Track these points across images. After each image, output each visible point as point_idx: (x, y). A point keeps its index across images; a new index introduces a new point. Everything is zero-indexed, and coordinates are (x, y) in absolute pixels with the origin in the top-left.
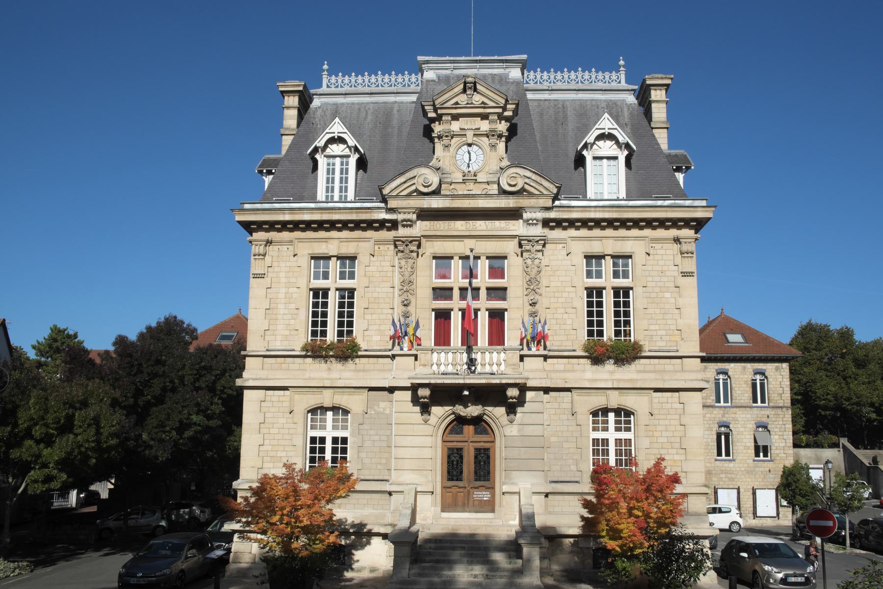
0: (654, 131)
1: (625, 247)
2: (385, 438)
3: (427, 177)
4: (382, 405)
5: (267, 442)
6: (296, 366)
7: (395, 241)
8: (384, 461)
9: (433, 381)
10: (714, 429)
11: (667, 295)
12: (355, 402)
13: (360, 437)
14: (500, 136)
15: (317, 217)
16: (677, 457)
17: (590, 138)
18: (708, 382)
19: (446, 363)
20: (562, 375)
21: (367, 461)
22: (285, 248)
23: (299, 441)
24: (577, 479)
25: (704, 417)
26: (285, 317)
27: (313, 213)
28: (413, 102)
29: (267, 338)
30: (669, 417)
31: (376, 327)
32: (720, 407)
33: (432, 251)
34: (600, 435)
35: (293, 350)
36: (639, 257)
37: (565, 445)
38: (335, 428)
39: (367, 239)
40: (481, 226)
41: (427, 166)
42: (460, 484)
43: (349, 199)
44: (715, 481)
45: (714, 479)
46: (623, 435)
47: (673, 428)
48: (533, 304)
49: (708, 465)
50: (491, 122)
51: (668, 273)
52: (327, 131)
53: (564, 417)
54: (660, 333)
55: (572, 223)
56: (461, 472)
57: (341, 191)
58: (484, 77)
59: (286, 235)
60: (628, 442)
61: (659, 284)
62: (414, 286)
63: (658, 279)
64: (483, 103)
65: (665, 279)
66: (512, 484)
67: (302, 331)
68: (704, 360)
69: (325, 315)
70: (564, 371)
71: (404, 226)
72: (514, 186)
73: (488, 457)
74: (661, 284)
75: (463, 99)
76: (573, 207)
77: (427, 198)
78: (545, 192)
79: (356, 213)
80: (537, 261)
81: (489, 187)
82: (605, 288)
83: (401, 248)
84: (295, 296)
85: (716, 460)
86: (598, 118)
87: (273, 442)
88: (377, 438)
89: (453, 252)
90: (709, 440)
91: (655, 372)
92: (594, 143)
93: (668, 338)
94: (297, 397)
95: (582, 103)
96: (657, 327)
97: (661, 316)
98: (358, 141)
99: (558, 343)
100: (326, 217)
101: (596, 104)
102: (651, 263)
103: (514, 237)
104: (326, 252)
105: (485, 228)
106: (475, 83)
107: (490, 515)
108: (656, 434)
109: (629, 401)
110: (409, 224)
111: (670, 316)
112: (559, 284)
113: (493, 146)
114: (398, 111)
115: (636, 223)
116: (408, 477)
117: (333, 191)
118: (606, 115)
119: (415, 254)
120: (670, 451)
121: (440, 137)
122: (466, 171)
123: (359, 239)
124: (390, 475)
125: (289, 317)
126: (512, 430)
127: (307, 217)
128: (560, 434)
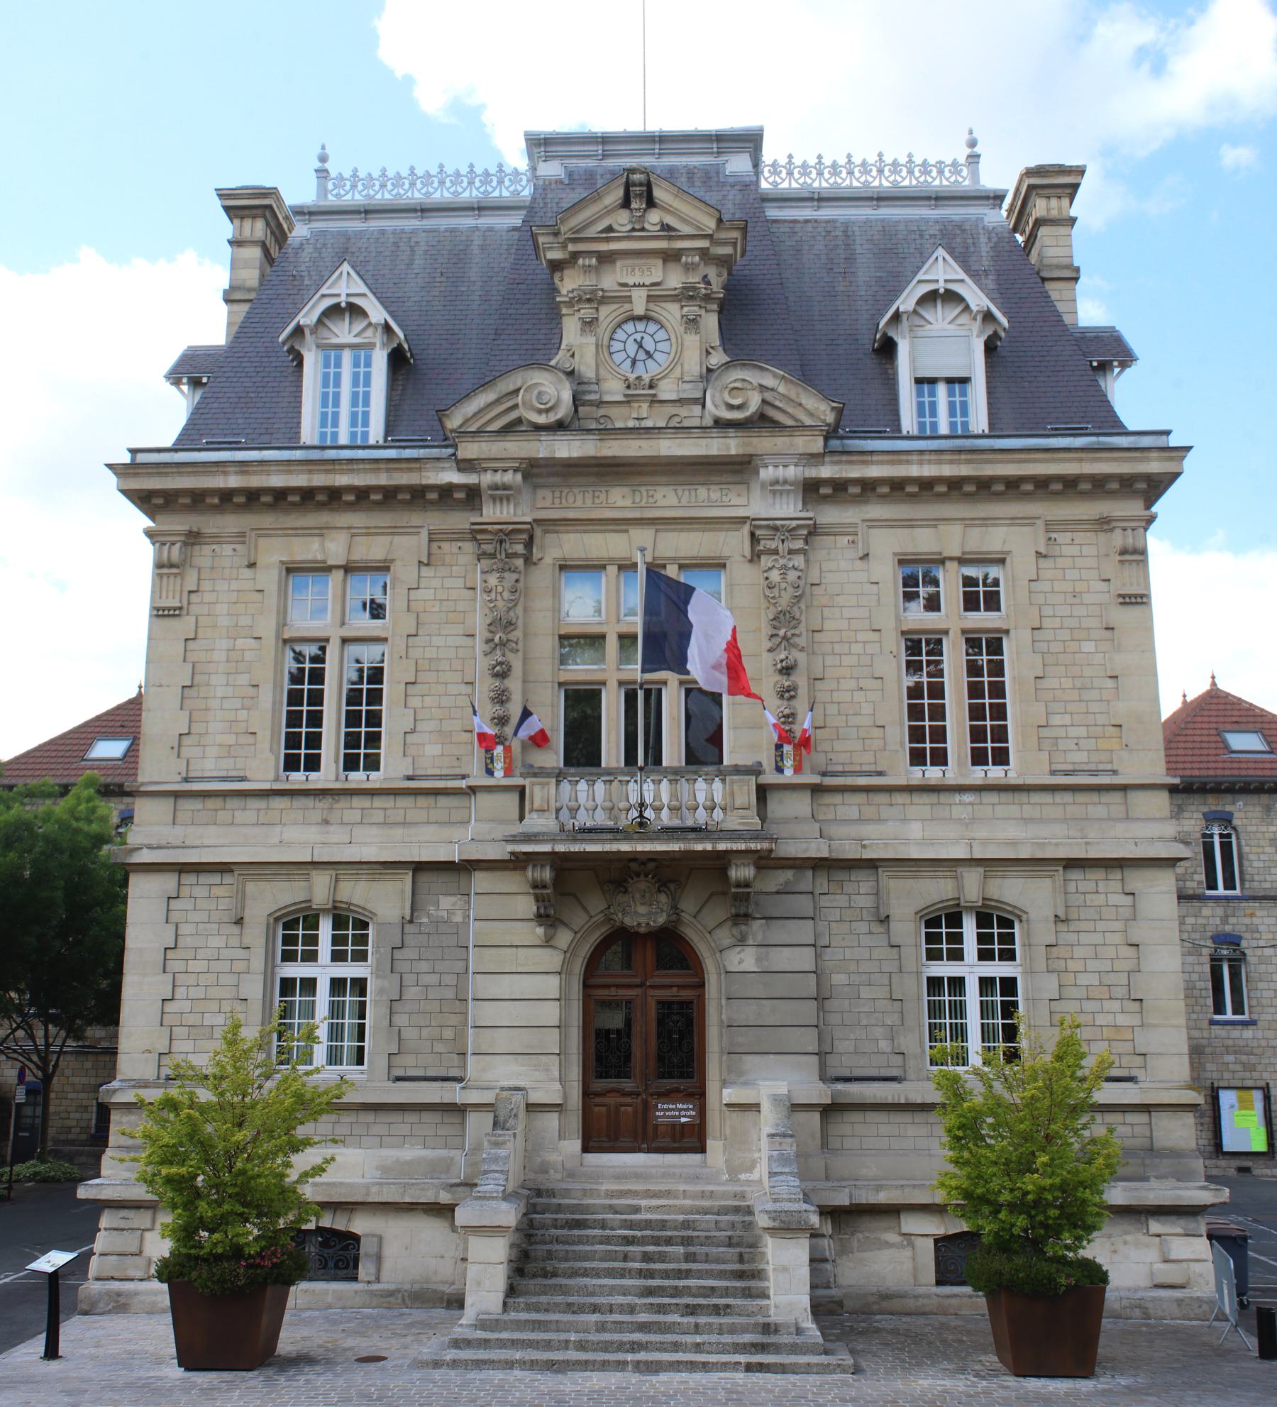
0: (1048, 285)
1: (994, 540)
2: (450, 980)
3: (548, 390)
4: (446, 902)
5: (180, 992)
6: (250, 816)
7: (473, 532)
8: (448, 1034)
9: (561, 848)
10: (1206, 951)
11: (1088, 647)
12: (385, 902)
14: (708, 298)
15: (299, 480)
16: (1122, 1020)
17: (906, 302)
18: (1186, 843)
19: (590, 804)
20: (853, 830)
21: (408, 1034)
22: (227, 549)
23: (254, 988)
24: (894, 1073)
25: (1182, 923)
26: (226, 704)
27: (290, 472)
28: (515, 229)
29: (185, 752)
30: (1101, 926)
31: (433, 725)
32: (1218, 899)
33: (557, 553)
34: (944, 969)
35: (243, 779)
36: (1022, 563)
37: (865, 993)
38: (337, 957)
39: (414, 530)
40: (666, 499)
41: (543, 365)
42: (628, 1085)
43: (372, 442)
44: (1212, 1071)
45: (1209, 1066)
46: (998, 969)
47: (1111, 952)
48: (787, 670)
49: (1196, 1034)
50: (688, 268)
51: (1088, 598)
52: (324, 291)
53: (862, 927)
54: (1073, 732)
55: (868, 488)
56: (628, 1058)
57: (354, 423)
58: (670, 176)
59: (230, 523)
60: (1009, 985)
61: (1069, 622)
62: (518, 634)
63: (1065, 611)
64: (666, 227)
65: (1081, 611)
66: (746, 1084)
67: (265, 736)
68: (1173, 790)
69: (317, 698)
70: (860, 820)
71: (494, 498)
72: (739, 407)
73: (690, 1023)
74: (1073, 623)
75: (622, 220)
76: (872, 452)
77: (544, 436)
78: (808, 422)
79: (388, 470)
80: (792, 576)
81: (683, 411)
82: (946, 632)
83: (489, 548)
84: (248, 656)
85: (1212, 1023)
86: (922, 257)
87: (194, 993)
88: (434, 979)
89: (605, 555)
90: (1195, 977)
91: (1065, 820)
92: (915, 312)
93: (1091, 743)
94: (251, 887)
95: (887, 229)
96: (1067, 720)
97: (1075, 695)
98: (391, 313)
99: (843, 758)
100: (319, 480)
101: (918, 230)
102: (1048, 574)
103: (743, 520)
104: (319, 557)
105: (674, 502)
106: (649, 185)
107: (697, 1157)
108: (1072, 965)
109: (1011, 891)
110: (502, 493)
111: (1094, 695)
112: (843, 625)
113: (692, 323)
114: (482, 248)
115: (1013, 486)
117: (336, 423)
118: (941, 252)
119: (519, 562)
120: (1108, 1005)
121: (570, 304)
122: (632, 377)
123: (394, 530)
124: (464, 1066)
125: (237, 703)
126: (744, 960)
127: (277, 481)
128: (853, 968)
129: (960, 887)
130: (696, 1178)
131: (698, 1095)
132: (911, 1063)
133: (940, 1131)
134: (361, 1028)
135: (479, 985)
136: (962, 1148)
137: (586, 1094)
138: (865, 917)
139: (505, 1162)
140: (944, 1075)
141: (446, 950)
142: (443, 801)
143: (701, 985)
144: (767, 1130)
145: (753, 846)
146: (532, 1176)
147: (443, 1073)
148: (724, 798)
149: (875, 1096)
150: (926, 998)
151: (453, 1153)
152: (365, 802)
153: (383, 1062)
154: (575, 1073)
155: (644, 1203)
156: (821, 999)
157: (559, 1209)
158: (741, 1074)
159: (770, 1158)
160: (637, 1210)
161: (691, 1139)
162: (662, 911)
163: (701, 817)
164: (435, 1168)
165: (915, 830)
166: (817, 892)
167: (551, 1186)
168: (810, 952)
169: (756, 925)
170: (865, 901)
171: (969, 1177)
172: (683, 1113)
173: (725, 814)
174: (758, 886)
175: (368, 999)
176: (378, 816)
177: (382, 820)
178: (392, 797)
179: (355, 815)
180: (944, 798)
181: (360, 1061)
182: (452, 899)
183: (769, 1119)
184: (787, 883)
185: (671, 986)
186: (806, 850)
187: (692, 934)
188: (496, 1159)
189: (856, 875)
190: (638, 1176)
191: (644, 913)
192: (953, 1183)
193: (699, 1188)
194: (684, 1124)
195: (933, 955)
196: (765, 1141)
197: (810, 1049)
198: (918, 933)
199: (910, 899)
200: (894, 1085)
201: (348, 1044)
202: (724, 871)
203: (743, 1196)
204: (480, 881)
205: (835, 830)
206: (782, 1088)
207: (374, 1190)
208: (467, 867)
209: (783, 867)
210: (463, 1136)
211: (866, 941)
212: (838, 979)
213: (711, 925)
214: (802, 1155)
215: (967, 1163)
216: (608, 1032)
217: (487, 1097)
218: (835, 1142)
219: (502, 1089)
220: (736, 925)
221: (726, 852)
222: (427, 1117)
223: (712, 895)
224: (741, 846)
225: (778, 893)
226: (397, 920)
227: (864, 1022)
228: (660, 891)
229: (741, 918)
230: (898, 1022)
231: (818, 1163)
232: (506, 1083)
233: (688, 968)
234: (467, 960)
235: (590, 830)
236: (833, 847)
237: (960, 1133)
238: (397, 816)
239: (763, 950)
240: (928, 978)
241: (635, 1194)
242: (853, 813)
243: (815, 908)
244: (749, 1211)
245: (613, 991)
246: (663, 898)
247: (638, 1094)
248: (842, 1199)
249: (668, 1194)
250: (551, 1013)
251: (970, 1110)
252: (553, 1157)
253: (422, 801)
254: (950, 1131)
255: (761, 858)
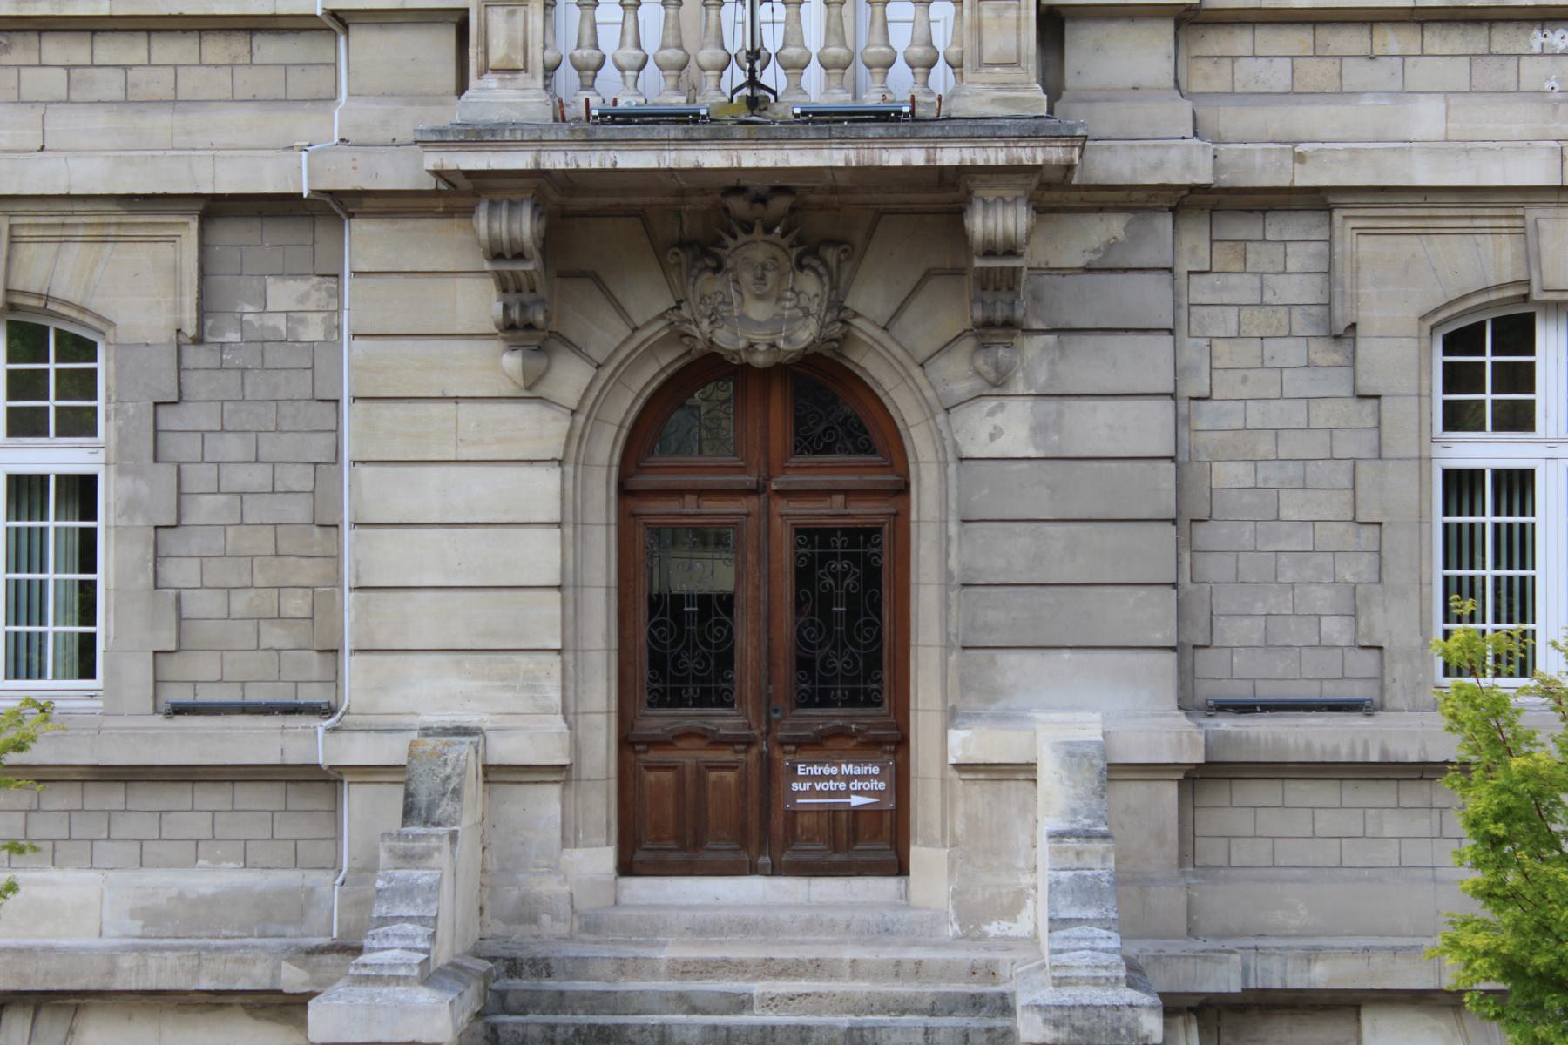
2: (298, 478)
4: (283, 294)
8: (296, 604)
9: (556, 160)
12: (132, 293)
13: (167, 473)
19: (629, 55)
20: (1277, 119)
21: (201, 604)
24: (1356, 692)
37: (1293, 506)
42: (725, 721)
53: (1290, 352)
56: (727, 660)
66: (1004, 718)
70: (1293, 94)
73: (872, 576)
88: (257, 477)
107: (885, 886)
116: (433, 695)
124: (335, 679)
126: (1005, 429)
128: (1265, 447)
129: (1531, 257)
130: (883, 933)
131: (892, 745)
132: (1398, 670)
133: (1456, 824)
134: (88, 589)
135: (367, 492)
136: (1503, 864)
137: (628, 742)
138: (1297, 329)
139: (433, 897)
140: (1470, 700)
141: (287, 409)
142: (269, 48)
143: (902, 490)
144: (1051, 821)
145: (1027, 154)
146: (498, 928)
147: (284, 695)
148: (957, 37)
149: (1309, 745)
150: (1439, 519)
151: (313, 877)
152: (73, 50)
153: (139, 671)
154: (600, 694)
155: (758, 988)
156: (1185, 521)
157: (560, 1002)
158: (992, 694)
159: (1054, 886)
160: (742, 1003)
161: (874, 844)
162: (807, 313)
163: (901, 85)
164: (269, 912)
165: (1427, 118)
166: (1184, 266)
167: (541, 951)
168: (1164, 408)
169: (1034, 348)
170: (1298, 289)
171: (1516, 927)
172: (856, 784)
173: (960, 77)
174: (1041, 253)
175: (100, 524)
176: (109, 85)
177: (118, 94)
178: (141, 39)
179: (54, 82)
180: (1504, 39)
181: (87, 671)
182: (301, 286)
183: (1057, 797)
184: (1110, 246)
185: (828, 493)
186: (1158, 166)
187: (875, 367)
188: (408, 892)
189: (1280, 227)
190: (746, 929)
191: (765, 318)
192: (1480, 942)
193: (889, 954)
194: (856, 812)
195: (1458, 418)
196: (1044, 844)
197: (1158, 638)
198: (1424, 366)
199: (1408, 284)
200: (1355, 721)
201: (56, 629)
202: (955, 215)
203: (992, 974)
204: (365, 242)
205: (1227, 118)
206: (1088, 728)
207: (126, 962)
208: (331, 208)
209: (1101, 209)
210: (337, 839)
211: (1298, 383)
212: (1229, 474)
213: (924, 349)
214: (1128, 881)
215: (1514, 897)
216: (678, 600)
217: (389, 751)
218: (1211, 852)
219: (427, 731)
220: (985, 346)
221: (960, 170)
222: (248, 796)
223: (928, 275)
224: (995, 155)
225: (1087, 270)
226: (165, 336)
227: (1289, 575)
228: (800, 266)
229: (998, 329)
230: (1369, 574)
231: (1168, 900)
232: (435, 719)
233: (869, 449)
234: (337, 431)
235: (628, 118)
236: (1222, 159)
237: (1500, 830)
238: (158, 83)
239: (1052, 405)
240: (1447, 473)
241: (739, 968)
242: (1277, 75)
243: (1176, 306)
244: (1004, 1006)
245: (690, 504)
246: (809, 284)
247: (749, 743)
248: (1226, 979)
249: (816, 968)
250: (541, 556)
251: (1527, 775)
252: (548, 887)
253: (217, 48)
254: (1475, 824)
255: (1046, 186)
